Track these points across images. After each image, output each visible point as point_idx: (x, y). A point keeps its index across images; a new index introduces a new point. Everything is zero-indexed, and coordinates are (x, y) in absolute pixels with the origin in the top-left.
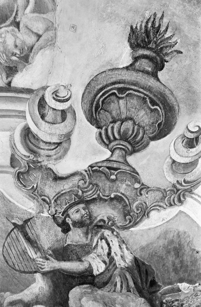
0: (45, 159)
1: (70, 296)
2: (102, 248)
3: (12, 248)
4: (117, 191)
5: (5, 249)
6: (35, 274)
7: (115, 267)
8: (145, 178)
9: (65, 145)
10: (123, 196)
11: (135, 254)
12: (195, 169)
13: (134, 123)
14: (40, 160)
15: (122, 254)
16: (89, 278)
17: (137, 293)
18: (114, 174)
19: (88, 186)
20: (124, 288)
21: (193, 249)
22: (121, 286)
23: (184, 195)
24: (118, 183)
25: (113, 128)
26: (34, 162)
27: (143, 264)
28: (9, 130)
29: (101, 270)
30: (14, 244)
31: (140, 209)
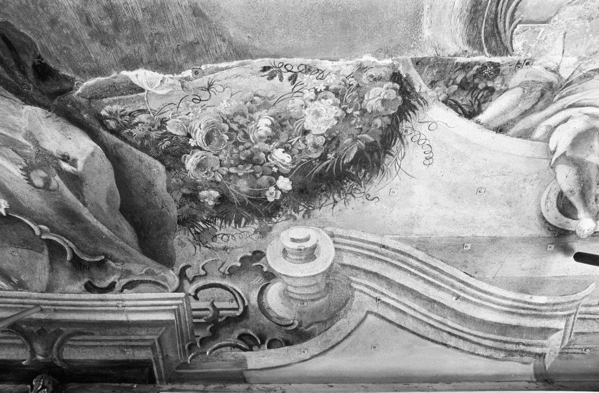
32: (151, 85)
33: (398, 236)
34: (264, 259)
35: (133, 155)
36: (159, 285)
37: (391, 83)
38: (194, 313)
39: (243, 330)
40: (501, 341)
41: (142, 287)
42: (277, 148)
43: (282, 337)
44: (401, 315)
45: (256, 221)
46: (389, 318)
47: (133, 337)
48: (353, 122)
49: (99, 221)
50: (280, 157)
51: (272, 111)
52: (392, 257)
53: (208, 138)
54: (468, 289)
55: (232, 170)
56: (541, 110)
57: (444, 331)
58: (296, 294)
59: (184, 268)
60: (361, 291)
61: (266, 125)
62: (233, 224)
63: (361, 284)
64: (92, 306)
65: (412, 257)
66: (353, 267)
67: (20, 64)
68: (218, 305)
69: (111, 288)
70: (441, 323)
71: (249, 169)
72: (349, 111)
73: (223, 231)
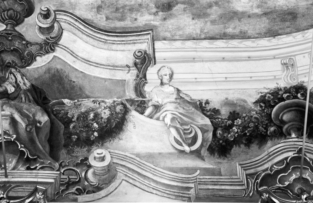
2: (12, 79)
4: (14, 46)
7: (20, 89)
8: (28, 38)
10: (18, 49)
11: (32, 82)
12: (54, 30)
13: (14, 11)
15: (24, 82)
16: (7, 95)
17: (35, 103)
18: (10, 37)
20: (27, 100)
21: (70, 80)
22: (25, 99)
23: (53, 46)
25: (4, 14)
27: (38, 88)
31: (29, 55)
32: (67, 103)
33: (130, 153)
34: (88, 160)
36: (53, 169)
37: (121, 105)
38: (62, 180)
39: (78, 187)
40: (172, 192)
41: (46, 169)
42: (95, 123)
43: (92, 189)
44: (134, 181)
45: (87, 147)
46: (130, 182)
48: (114, 115)
50: (95, 125)
51: (94, 112)
52: (129, 160)
53: (77, 119)
54: (156, 171)
55: (82, 129)
56: (159, 112)
57: (151, 187)
58: (98, 173)
59: (62, 162)
60: (120, 172)
61: (92, 116)
62: (80, 148)
63: (119, 169)
65: (135, 160)
66: (116, 163)
67: (41, 96)
68: (70, 177)
69: (35, 169)
70: (149, 184)
71: (87, 129)
72: (113, 112)
73: (76, 150)
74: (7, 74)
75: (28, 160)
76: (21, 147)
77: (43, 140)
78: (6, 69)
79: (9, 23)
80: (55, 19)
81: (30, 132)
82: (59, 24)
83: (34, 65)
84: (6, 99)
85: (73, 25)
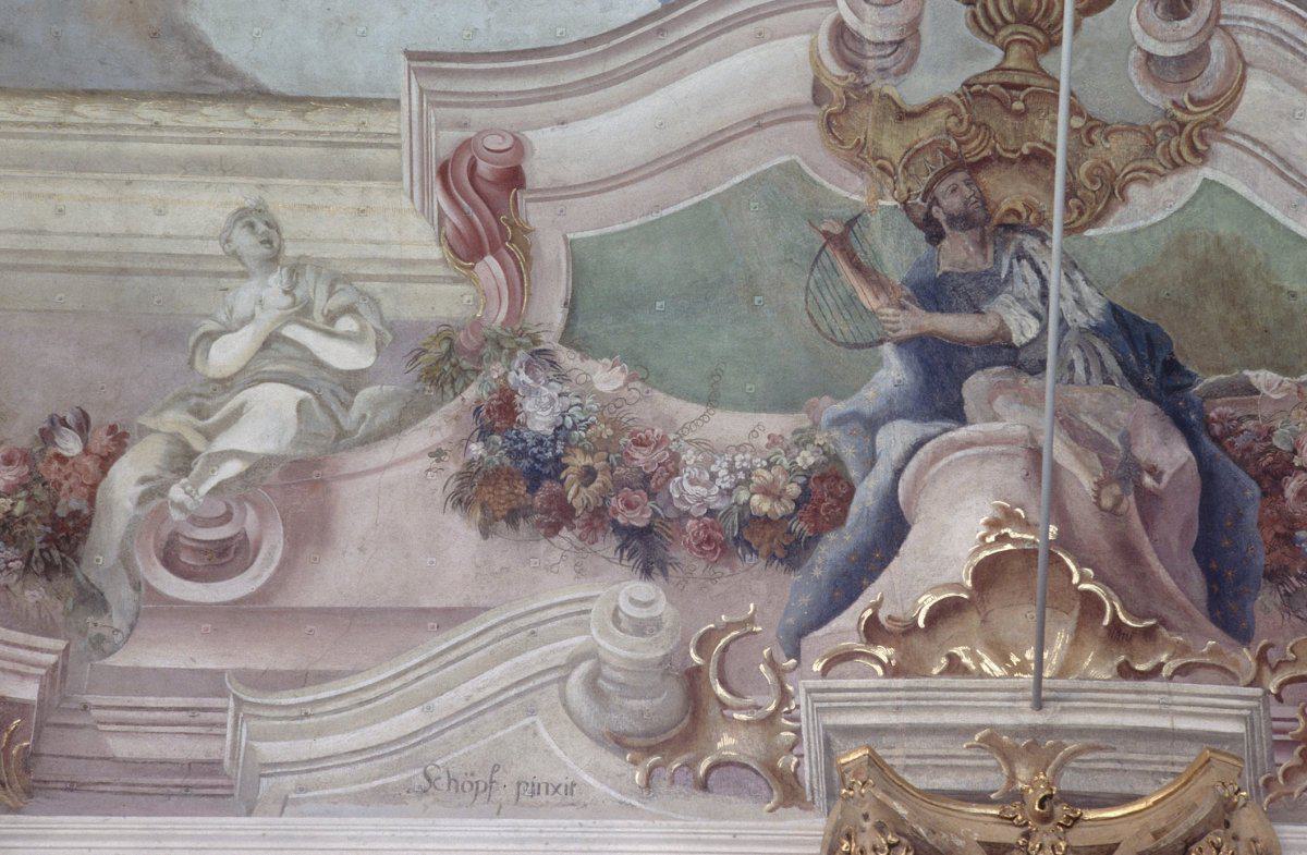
0: (875, 75)
1: (966, 393)
3: (825, 291)
4: (1034, 138)
5: (810, 298)
6: (880, 347)
9: (910, 44)
12: (1208, 69)
14: (867, 80)
19: (968, 131)
21: (1275, 286)
22: (1087, 371)
23: (1202, 137)
24: (1031, 118)
26: (856, 87)
27: (1138, 320)
28: (808, 32)
29: (1031, 334)
30: (829, 282)
31: (1098, 179)
32: (1268, 387)
35: (1227, 466)
36: (1228, 674)
41: (1201, 673)
47: (1176, 758)
49: (1163, 564)
64: (1122, 702)
67: (1152, 355)
69: (1154, 673)
74: (1005, 262)
75: (1117, 632)
76: (1083, 579)
77: (1175, 550)
78: (998, 239)
79: (1014, 40)
80: (1213, 18)
81: (1113, 511)
82: (1229, 40)
83: (1120, 221)
84: (1004, 368)
85: (1292, 43)
